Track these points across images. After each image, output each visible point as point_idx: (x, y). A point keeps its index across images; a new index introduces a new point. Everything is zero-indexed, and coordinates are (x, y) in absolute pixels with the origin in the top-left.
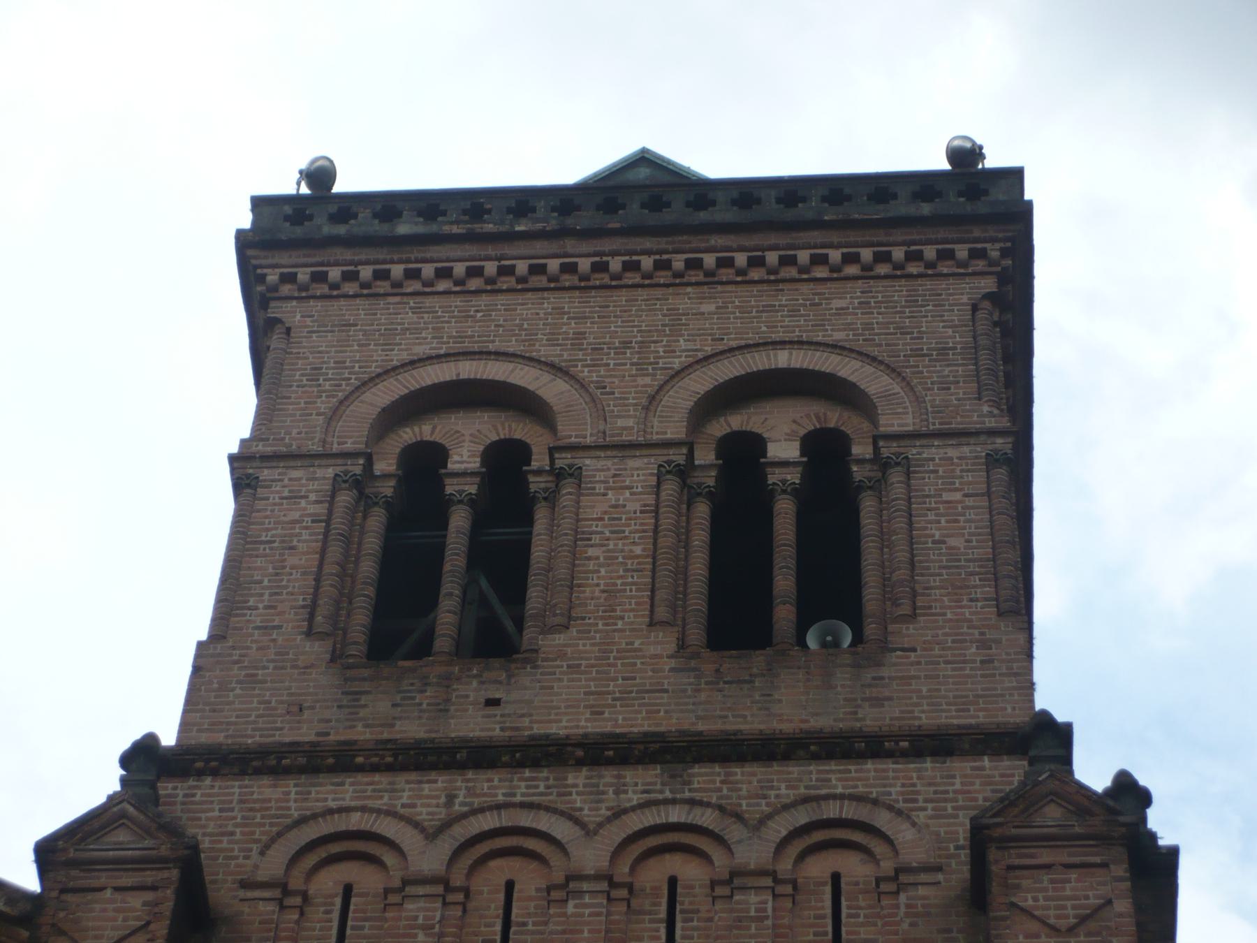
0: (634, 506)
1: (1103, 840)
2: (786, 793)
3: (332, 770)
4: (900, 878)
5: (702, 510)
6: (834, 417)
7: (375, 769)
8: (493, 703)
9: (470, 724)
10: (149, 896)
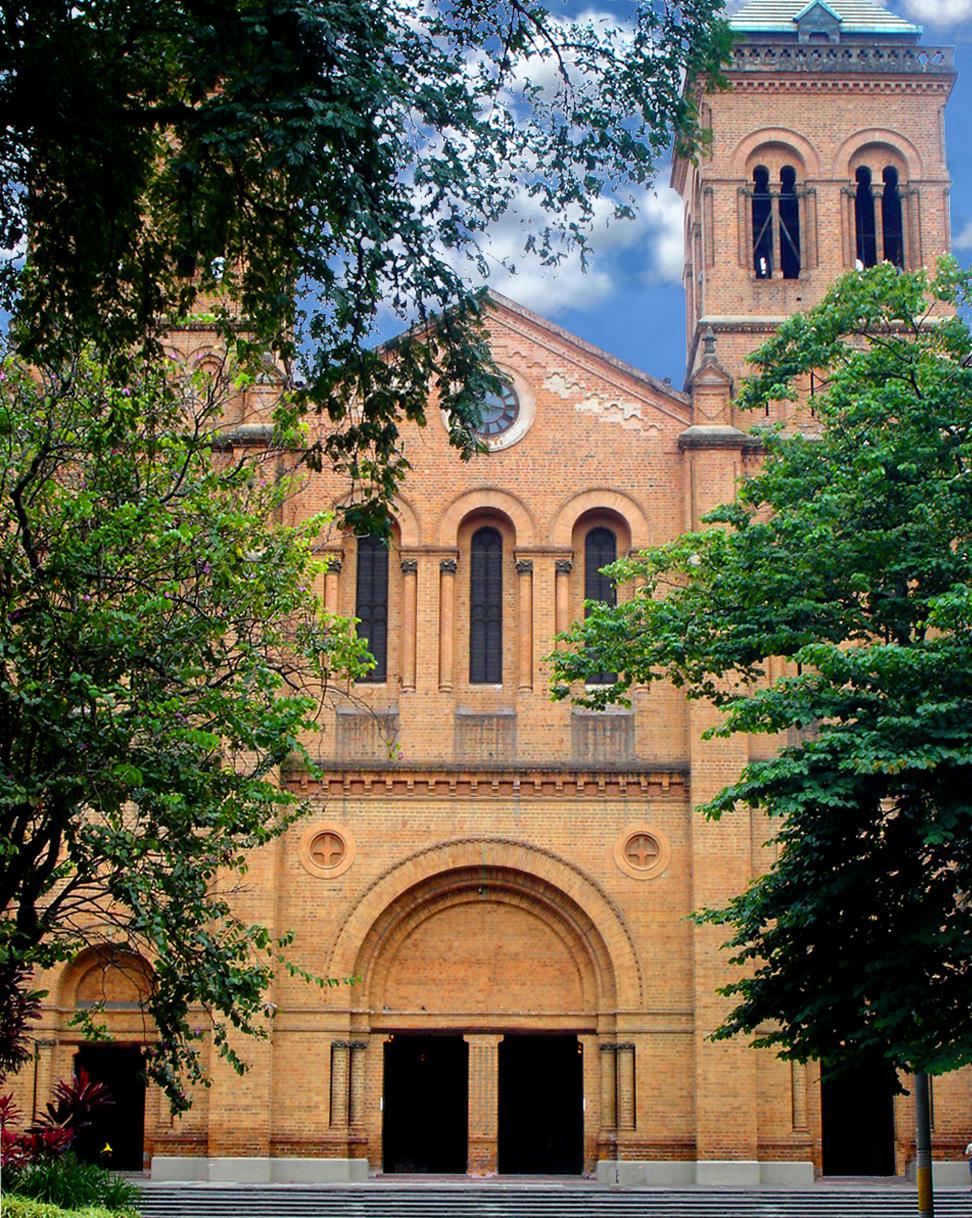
0: (834, 210)
5: (853, 202)
6: (894, 162)
8: (799, 299)
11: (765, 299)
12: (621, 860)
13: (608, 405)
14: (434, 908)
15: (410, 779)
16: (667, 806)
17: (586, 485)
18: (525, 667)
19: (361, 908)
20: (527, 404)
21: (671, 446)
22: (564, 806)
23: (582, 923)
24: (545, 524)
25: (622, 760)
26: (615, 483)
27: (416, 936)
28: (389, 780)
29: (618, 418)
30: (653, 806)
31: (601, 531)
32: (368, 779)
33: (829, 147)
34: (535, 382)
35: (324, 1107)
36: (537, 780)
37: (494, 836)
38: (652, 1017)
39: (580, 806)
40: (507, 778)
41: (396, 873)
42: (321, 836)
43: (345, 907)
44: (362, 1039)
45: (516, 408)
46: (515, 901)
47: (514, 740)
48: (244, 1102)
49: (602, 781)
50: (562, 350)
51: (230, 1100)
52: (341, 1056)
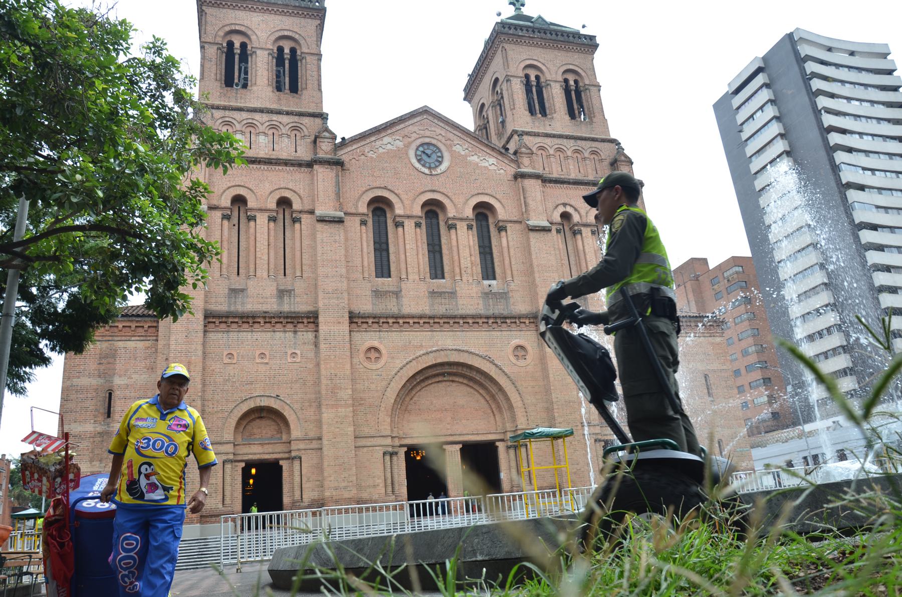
4: (601, 160)
11: (537, 124)
14: (423, 385)
15: (411, 321)
16: (529, 333)
17: (476, 192)
18: (457, 270)
19: (392, 384)
20: (446, 155)
21: (510, 177)
22: (483, 333)
23: (495, 388)
24: (460, 207)
25: (505, 313)
26: (489, 192)
27: (415, 399)
28: (401, 321)
29: (486, 164)
30: (523, 333)
31: (483, 211)
32: (391, 321)
33: (553, 69)
34: (449, 148)
35: (382, 485)
36: (471, 321)
37: (454, 347)
40: (457, 320)
41: (408, 366)
42: (370, 349)
43: (384, 383)
44: (396, 450)
45: (442, 157)
46: (461, 380)
47: (457, 305)
48: (343, 484)
49: (499, 321)
50: (460, 135)
51: (336, 484)
52: (388, 458)
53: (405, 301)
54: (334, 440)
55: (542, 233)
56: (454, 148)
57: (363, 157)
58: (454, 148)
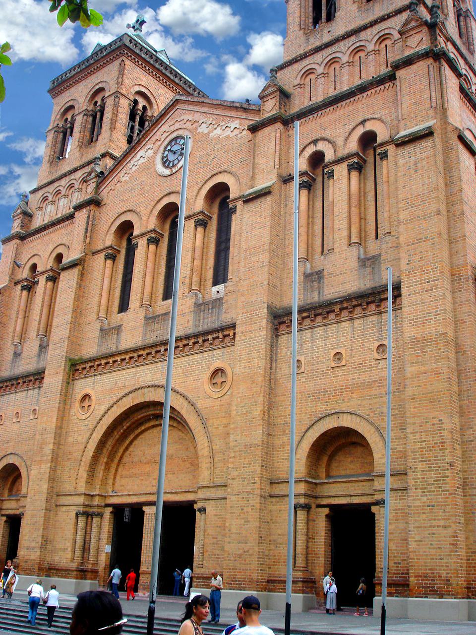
1: (421, 25)
2: (376, 32)
3: (305, 57)
7: (310, 55)
8: (329, 32)
9: (327, 38)
10: (275, 98)
12: (208, 388)
13: (224, 128)
30: (226, 350)
38: (215, 489)
39: (191, 357)
53: (123, 335)
54: (33, 498)
55: (259, 200)
56: (200, 130)
57: (119, 184)
58: (200, 130)
